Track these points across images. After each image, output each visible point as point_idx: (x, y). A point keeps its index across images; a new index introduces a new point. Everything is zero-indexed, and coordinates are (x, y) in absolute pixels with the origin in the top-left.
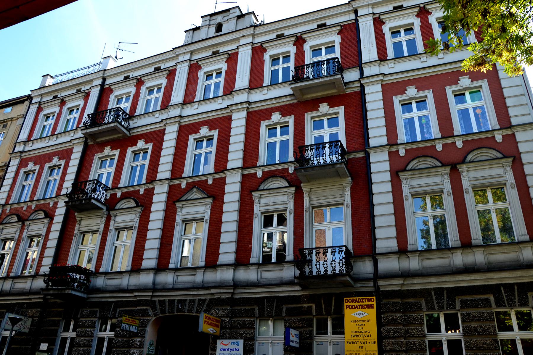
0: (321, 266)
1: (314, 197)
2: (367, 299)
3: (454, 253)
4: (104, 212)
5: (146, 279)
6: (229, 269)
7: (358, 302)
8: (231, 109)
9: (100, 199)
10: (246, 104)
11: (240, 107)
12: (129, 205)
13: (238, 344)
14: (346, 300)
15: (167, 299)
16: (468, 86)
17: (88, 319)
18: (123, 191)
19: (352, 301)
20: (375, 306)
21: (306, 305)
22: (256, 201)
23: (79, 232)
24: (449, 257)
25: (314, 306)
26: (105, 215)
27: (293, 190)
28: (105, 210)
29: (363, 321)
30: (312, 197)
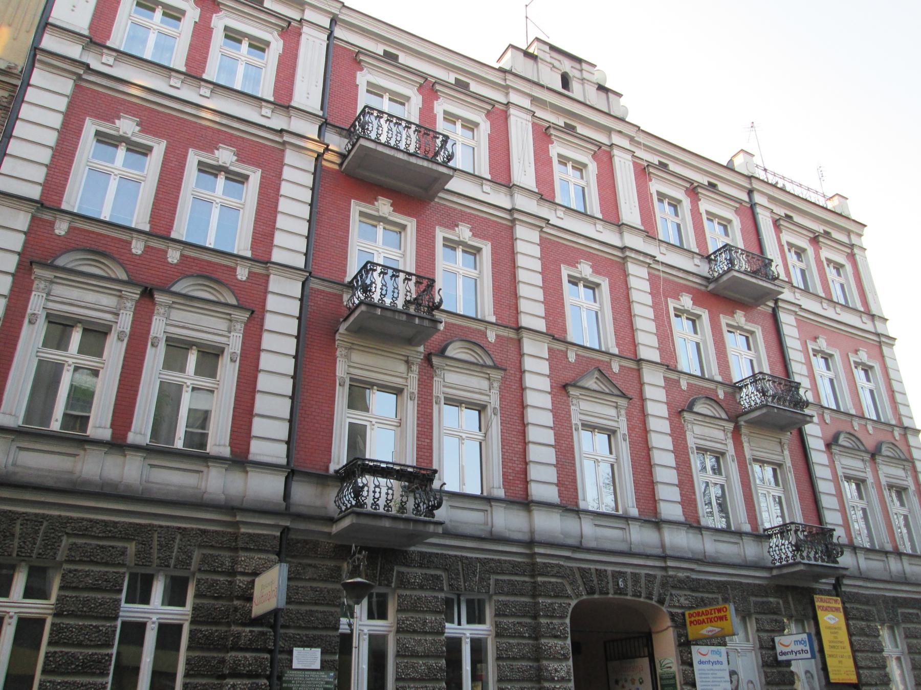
4: (418, 352)
11: (641, 258)
12: (469, 356)
13: (719, 653)
17: (423, 594)
20: (842, 610)
23: (349, 376)
25: (781, 602)
26: (419, 360)
29: (835, 628)
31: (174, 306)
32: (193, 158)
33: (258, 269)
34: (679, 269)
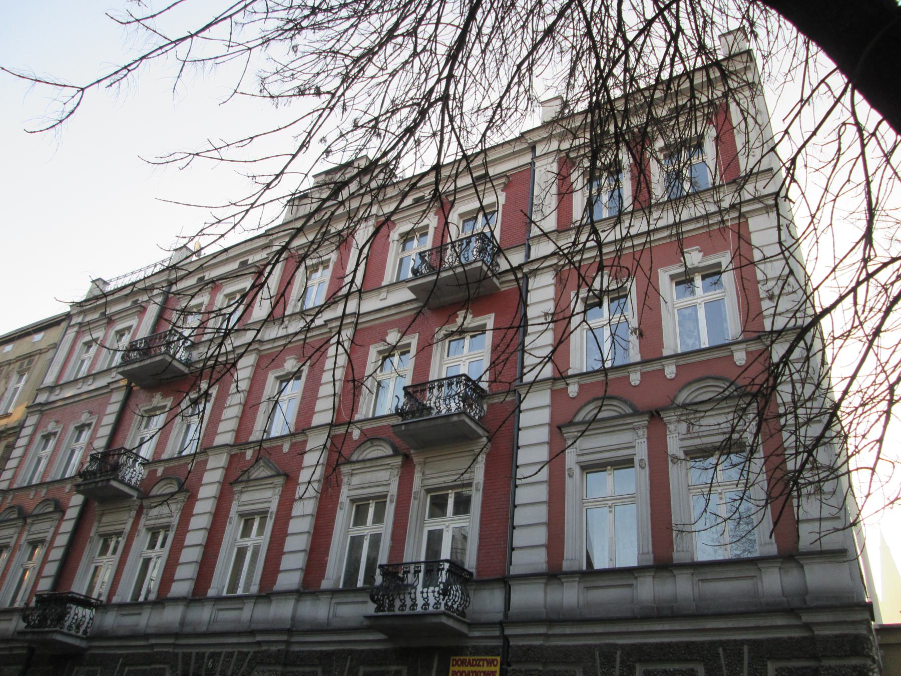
0: (419, 595)
1: (430, 472)
2: (486, 660)
3: (639, 577)
5: (171, 616)
6: (289, 599)
7: (472, 665)
8: (329, 326)
9: (130, 480)
10: (351, 318)
14: (453, 660)
15: (194, 651)
16: (696, 264)
18: (167, 466)
19: (463, 663)
21: (393, 668)
22: (345, 479)
24: (632, 585)
27: (398, 460)
28: (135, 498)
30: (427, 472)
31: (354, 472)
32: (664, 277)
33: (755, 347)
34: (389, 307)
